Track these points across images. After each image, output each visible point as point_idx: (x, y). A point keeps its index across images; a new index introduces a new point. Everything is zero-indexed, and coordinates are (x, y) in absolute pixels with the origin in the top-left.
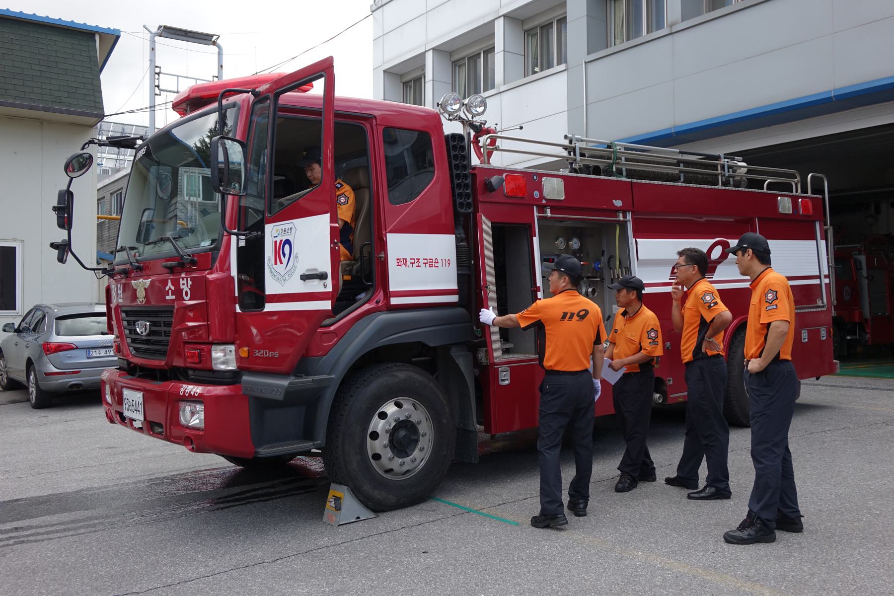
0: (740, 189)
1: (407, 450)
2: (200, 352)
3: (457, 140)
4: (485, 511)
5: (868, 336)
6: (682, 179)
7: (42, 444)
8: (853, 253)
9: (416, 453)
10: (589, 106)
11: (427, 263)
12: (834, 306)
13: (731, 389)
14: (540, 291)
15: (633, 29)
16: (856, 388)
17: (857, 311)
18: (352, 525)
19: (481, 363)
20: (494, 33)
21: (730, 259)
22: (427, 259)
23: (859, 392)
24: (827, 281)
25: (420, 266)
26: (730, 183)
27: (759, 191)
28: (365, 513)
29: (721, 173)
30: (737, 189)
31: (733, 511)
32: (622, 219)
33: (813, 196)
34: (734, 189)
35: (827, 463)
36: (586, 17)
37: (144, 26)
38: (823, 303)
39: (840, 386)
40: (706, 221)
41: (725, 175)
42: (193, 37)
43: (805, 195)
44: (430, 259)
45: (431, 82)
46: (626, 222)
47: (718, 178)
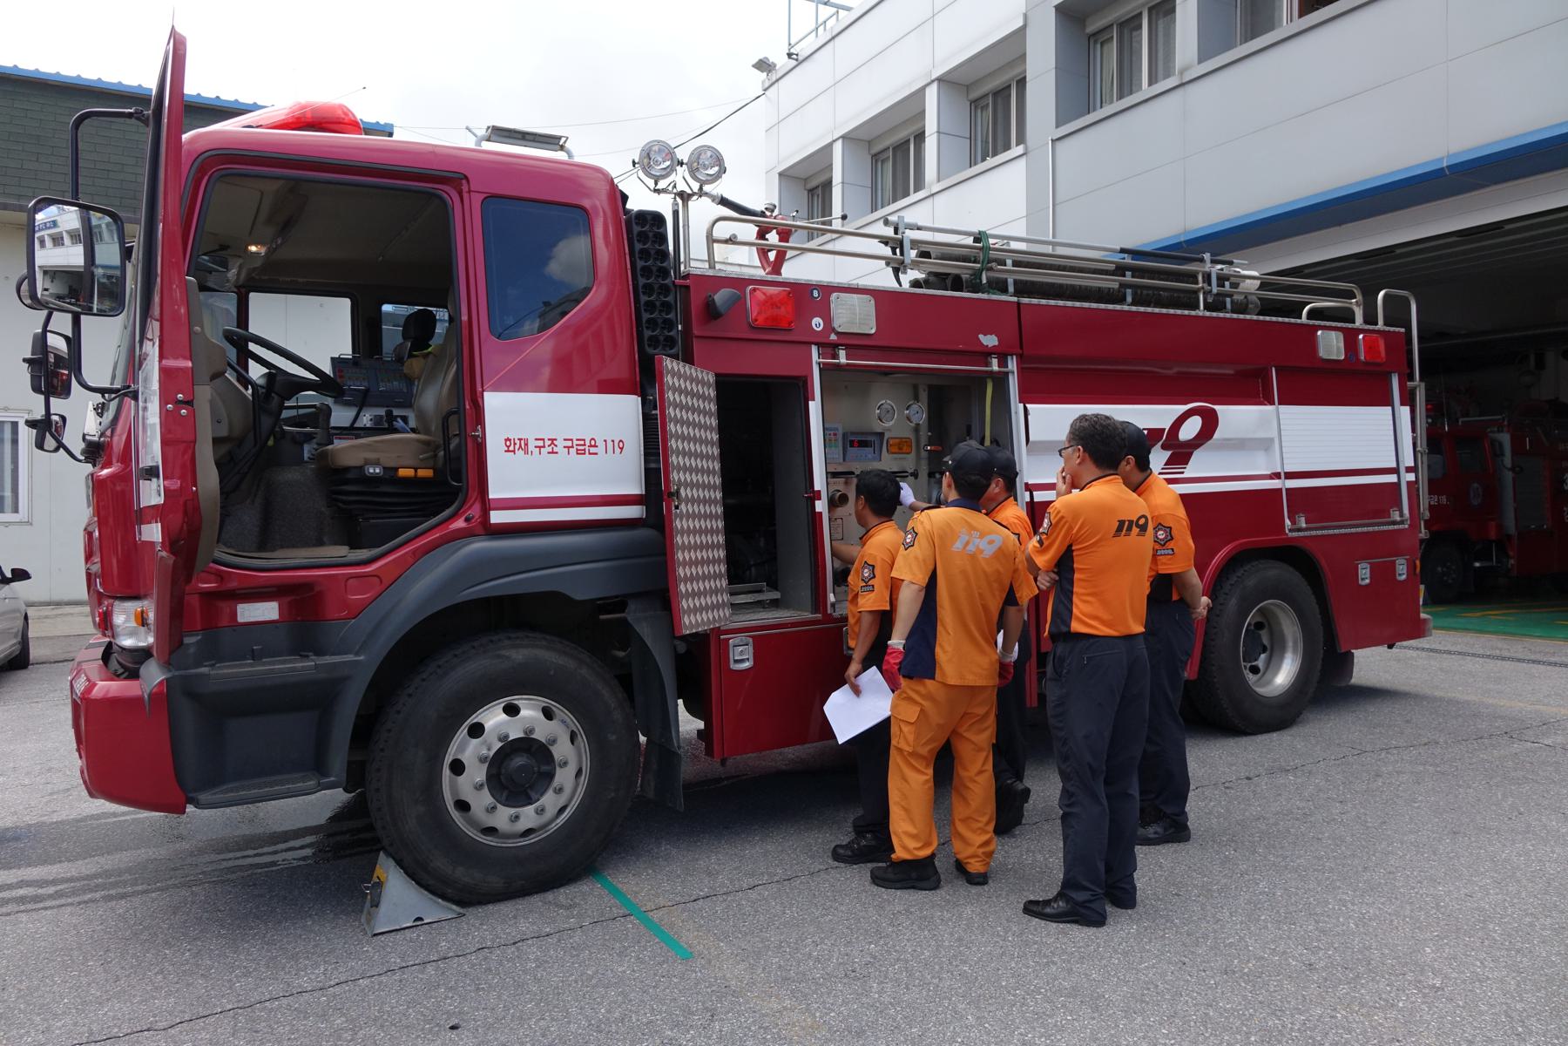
0: (1248, 317)
4: (656, 916)
5: (1512, 561)
6: (1129, 299)
8: (1489, 430)
9: (549, 800)
10: (1058, 208)
11: (572, 447)
12: (1426, 521)
14: (820, 499)
15: (1127, 84)
16: (1474, 655)
17: (1493, 523)
20: (924, 111)
21: (1217, 440)
23: (1471, 665)
24: (1411, 477)
25: (557, 453)
26: (1225, 308)
27: (1293, 320)
28: (434, 909)
29: (1203, 288)
30: (1241, 316)
31: (1125, 954)
32: (995, 368)
33: (1387, 329)
35: (1368, 827)
36: (1054, 71)
37: (467, 128)
38: (1401, 515)
39: (1445, 652)
40: (1179, 373)
41: (1211, 291)
42: (534, 141)
43: (1371, 327)
44: (578, 440)
45: (840, 186)
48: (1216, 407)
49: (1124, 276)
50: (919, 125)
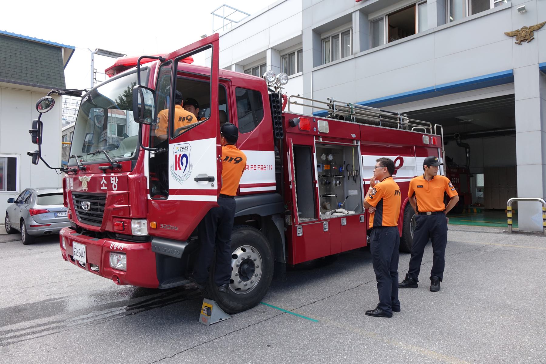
1: (248, 277)
2: (124, 224)
3: (275, 97)
4: (294, 311)
6: (381, 125)
7: (26, 268)
9: (253, 278)
10: (314, 93)
13: (404, 234)
14: (317, 183)
18: (218, 324)
19: (287, 224)
22: (260, 165)
28: (225, 317)
30: (404, 130)
32: (356, 144)
34: (403, 130)
36: (312, 50)
37: (88, 49)
40: (391, 147)
43: (434, 135)
44: (261, 165)
46: (357, 146)
47: (398, 125)
48: (403, 157)
49: (379, 117)
50: (264, 61)
